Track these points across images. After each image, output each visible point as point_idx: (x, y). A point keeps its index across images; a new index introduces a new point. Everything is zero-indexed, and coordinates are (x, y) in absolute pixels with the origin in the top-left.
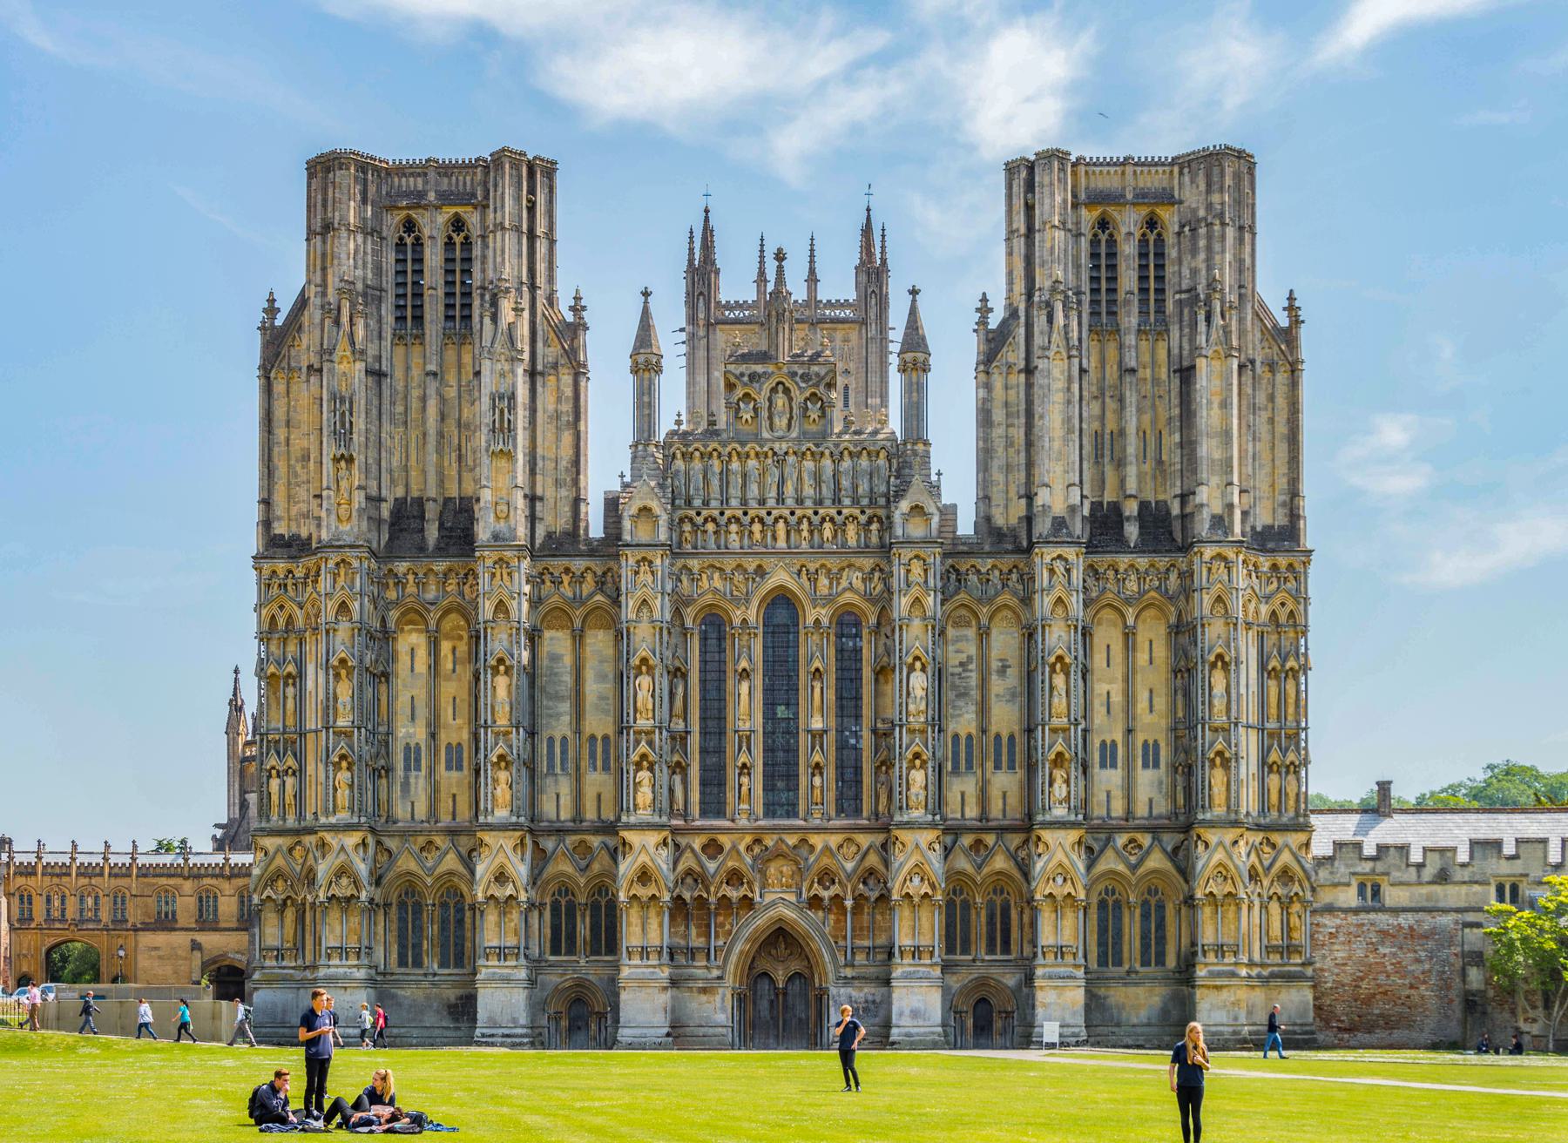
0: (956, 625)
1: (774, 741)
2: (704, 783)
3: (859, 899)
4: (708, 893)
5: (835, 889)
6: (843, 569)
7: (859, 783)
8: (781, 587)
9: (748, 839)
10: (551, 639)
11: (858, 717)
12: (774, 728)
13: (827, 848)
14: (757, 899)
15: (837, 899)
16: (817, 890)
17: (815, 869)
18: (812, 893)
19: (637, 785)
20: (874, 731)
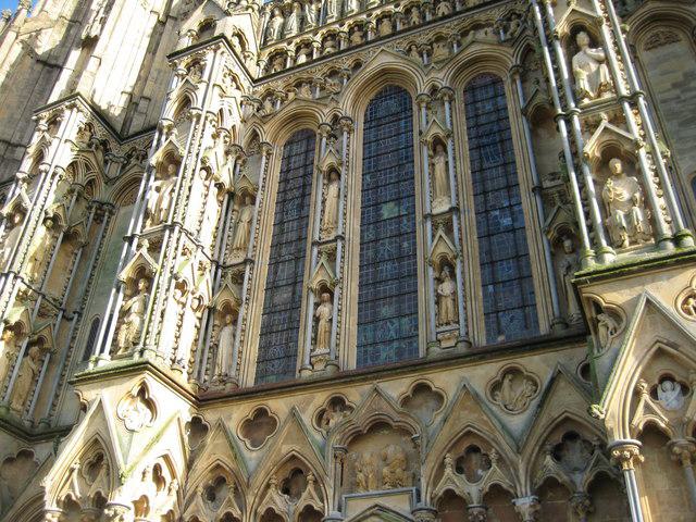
0: (653, 45)
1: (376, 252)
2: (266, 331)
3: (546, 489)
4: (242, 508)
5: (495, 475)
6: (465, 34)
7: (524, 277)
8: (384, 72)
9: (320, 398)
10: (125, 214)
11: (511, 187)
12: (377, 233)
13: (466, 389)
14: (330, 511)
15: (497, 494)
16: (454, 481)
17: (443, 437)
18: (440, 490)
19: (125, 313)
20: (538, 190)
